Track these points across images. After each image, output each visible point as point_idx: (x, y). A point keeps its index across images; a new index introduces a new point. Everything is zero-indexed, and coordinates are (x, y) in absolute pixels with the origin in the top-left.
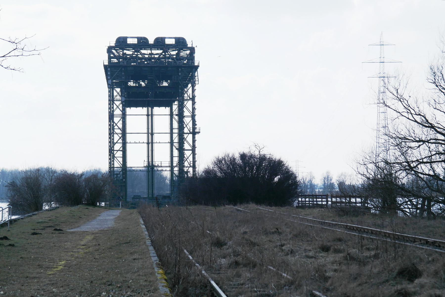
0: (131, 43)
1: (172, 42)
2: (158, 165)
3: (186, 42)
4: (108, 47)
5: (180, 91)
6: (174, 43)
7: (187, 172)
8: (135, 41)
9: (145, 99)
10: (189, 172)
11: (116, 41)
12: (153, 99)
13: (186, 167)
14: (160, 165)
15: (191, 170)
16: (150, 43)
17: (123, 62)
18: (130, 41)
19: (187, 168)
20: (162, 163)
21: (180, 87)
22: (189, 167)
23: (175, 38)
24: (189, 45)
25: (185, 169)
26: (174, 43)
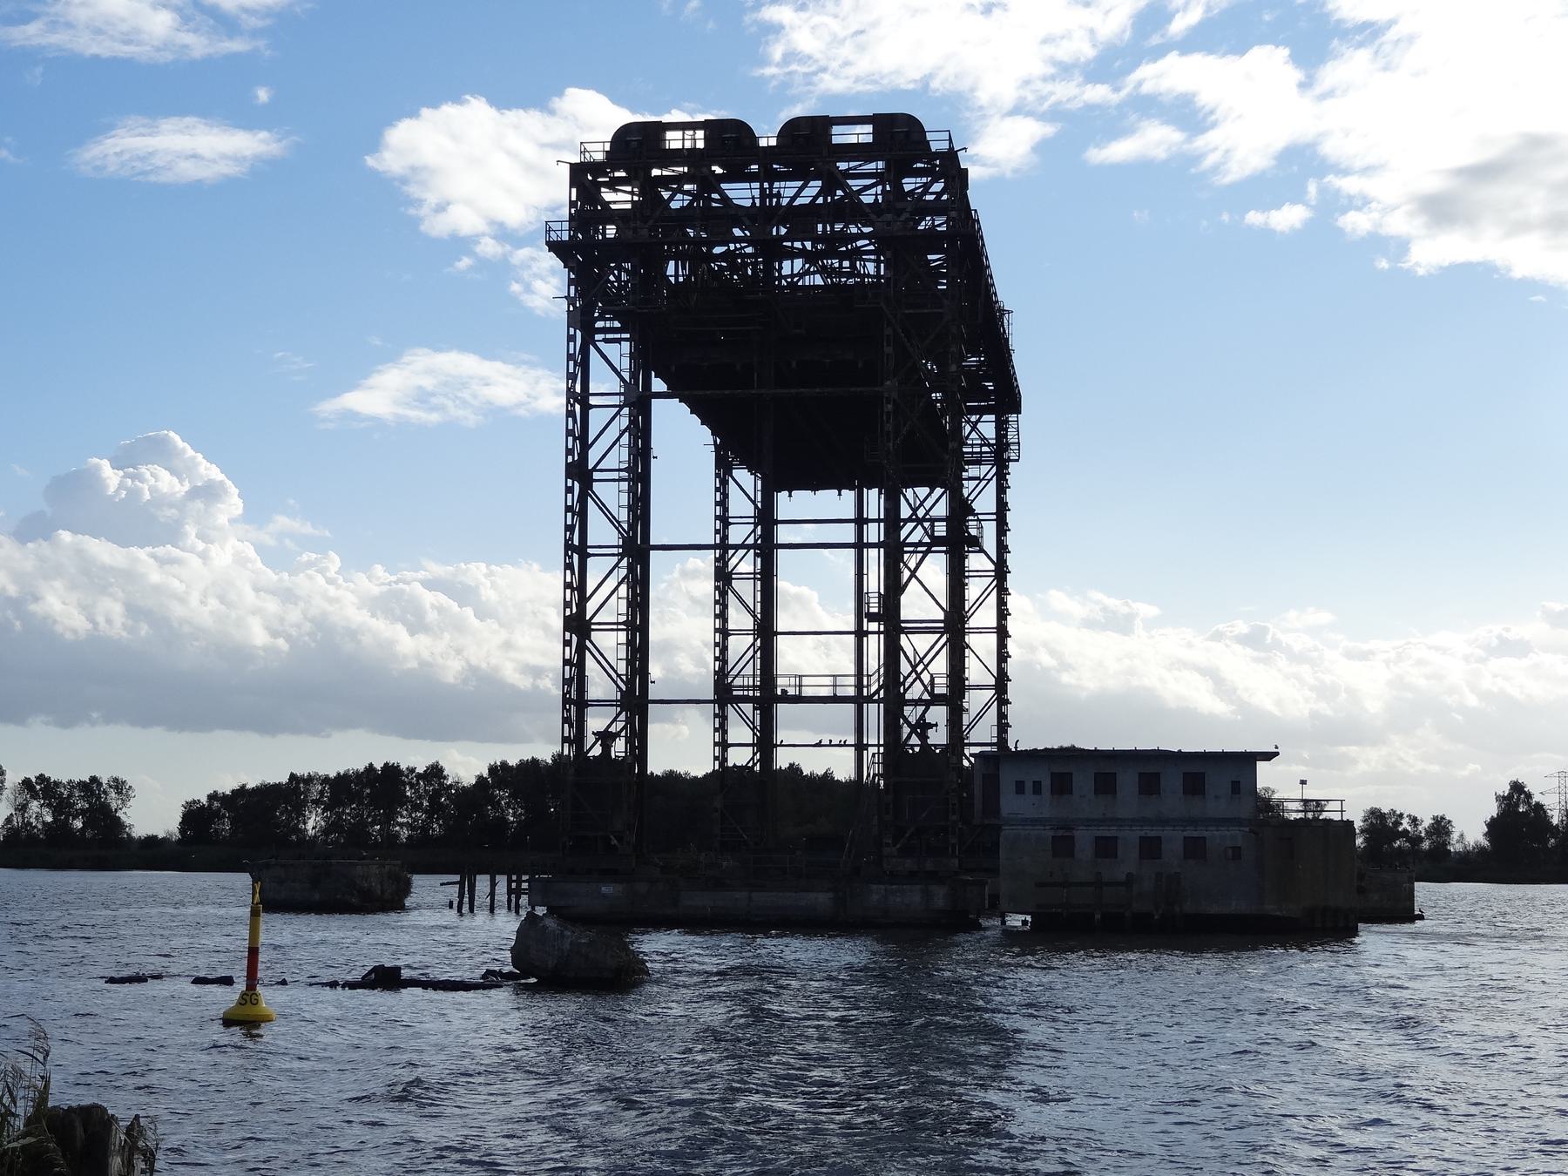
0: (676, 145)
1: (862, 134)
2: (784, 692)
3: (923, 132)
4: (573, 167)
5: (888, 350)
6: (869, 139)
7: (922, 727)
8: (699, 140)
9: (727, 392)
10: (931, 726)
11: (612, 142)
12: (763, 391)
13: (916, 703)
14: (791, 692)
15: (938, 714)
16: (763, 143)
17: (635, 230)
18: (674, 140)
19: (921, 709)
20: (805, 681)
21: (888, 331)
22: (928, 704)
23: (874, 120)
24: (937, 145)
25: (912, 714)
26: (869, 139)
